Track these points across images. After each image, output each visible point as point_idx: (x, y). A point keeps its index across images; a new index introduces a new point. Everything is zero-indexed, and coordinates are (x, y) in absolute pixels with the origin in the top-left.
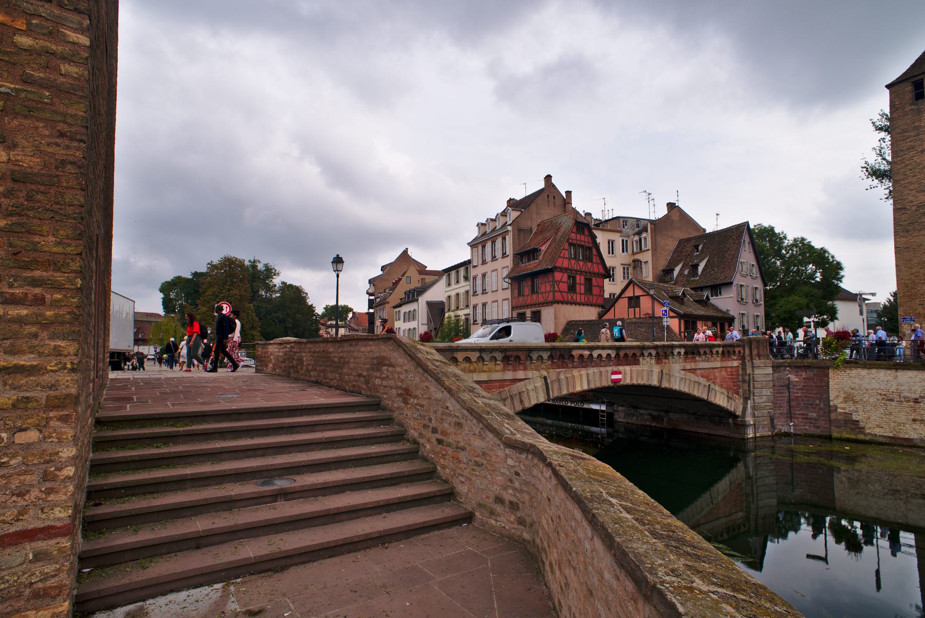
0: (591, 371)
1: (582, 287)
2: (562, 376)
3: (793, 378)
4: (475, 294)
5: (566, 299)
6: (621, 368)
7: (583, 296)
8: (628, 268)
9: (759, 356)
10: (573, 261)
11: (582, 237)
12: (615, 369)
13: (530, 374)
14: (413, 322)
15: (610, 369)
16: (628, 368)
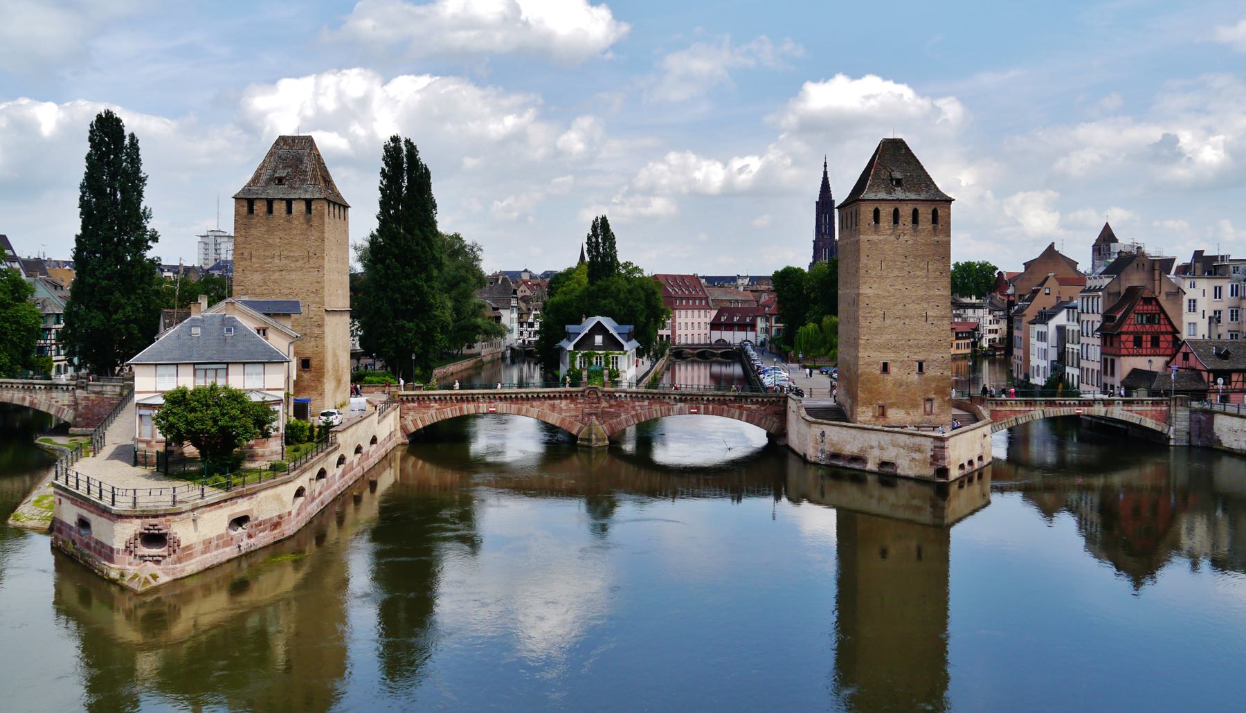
0: (1065, 409)
1: (1149, 344)
2: (1051, 411)
3: (1203, 418)
4: (1082, 335)
5: (1132, 353)
6: (1082, 408)
7: (1149, 350)
8: (1237, 311)
9: (1181, 405)
10: (1139, 326)
11: (1150, 307)
12: (1079, 408)
13: (1037, 408)
14: (1043, 343)
15: (1076, 408)
16: (1086, 408)
